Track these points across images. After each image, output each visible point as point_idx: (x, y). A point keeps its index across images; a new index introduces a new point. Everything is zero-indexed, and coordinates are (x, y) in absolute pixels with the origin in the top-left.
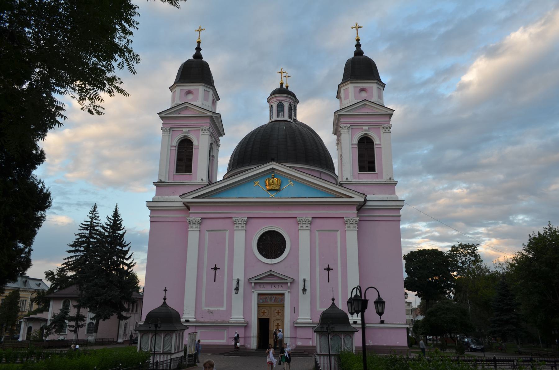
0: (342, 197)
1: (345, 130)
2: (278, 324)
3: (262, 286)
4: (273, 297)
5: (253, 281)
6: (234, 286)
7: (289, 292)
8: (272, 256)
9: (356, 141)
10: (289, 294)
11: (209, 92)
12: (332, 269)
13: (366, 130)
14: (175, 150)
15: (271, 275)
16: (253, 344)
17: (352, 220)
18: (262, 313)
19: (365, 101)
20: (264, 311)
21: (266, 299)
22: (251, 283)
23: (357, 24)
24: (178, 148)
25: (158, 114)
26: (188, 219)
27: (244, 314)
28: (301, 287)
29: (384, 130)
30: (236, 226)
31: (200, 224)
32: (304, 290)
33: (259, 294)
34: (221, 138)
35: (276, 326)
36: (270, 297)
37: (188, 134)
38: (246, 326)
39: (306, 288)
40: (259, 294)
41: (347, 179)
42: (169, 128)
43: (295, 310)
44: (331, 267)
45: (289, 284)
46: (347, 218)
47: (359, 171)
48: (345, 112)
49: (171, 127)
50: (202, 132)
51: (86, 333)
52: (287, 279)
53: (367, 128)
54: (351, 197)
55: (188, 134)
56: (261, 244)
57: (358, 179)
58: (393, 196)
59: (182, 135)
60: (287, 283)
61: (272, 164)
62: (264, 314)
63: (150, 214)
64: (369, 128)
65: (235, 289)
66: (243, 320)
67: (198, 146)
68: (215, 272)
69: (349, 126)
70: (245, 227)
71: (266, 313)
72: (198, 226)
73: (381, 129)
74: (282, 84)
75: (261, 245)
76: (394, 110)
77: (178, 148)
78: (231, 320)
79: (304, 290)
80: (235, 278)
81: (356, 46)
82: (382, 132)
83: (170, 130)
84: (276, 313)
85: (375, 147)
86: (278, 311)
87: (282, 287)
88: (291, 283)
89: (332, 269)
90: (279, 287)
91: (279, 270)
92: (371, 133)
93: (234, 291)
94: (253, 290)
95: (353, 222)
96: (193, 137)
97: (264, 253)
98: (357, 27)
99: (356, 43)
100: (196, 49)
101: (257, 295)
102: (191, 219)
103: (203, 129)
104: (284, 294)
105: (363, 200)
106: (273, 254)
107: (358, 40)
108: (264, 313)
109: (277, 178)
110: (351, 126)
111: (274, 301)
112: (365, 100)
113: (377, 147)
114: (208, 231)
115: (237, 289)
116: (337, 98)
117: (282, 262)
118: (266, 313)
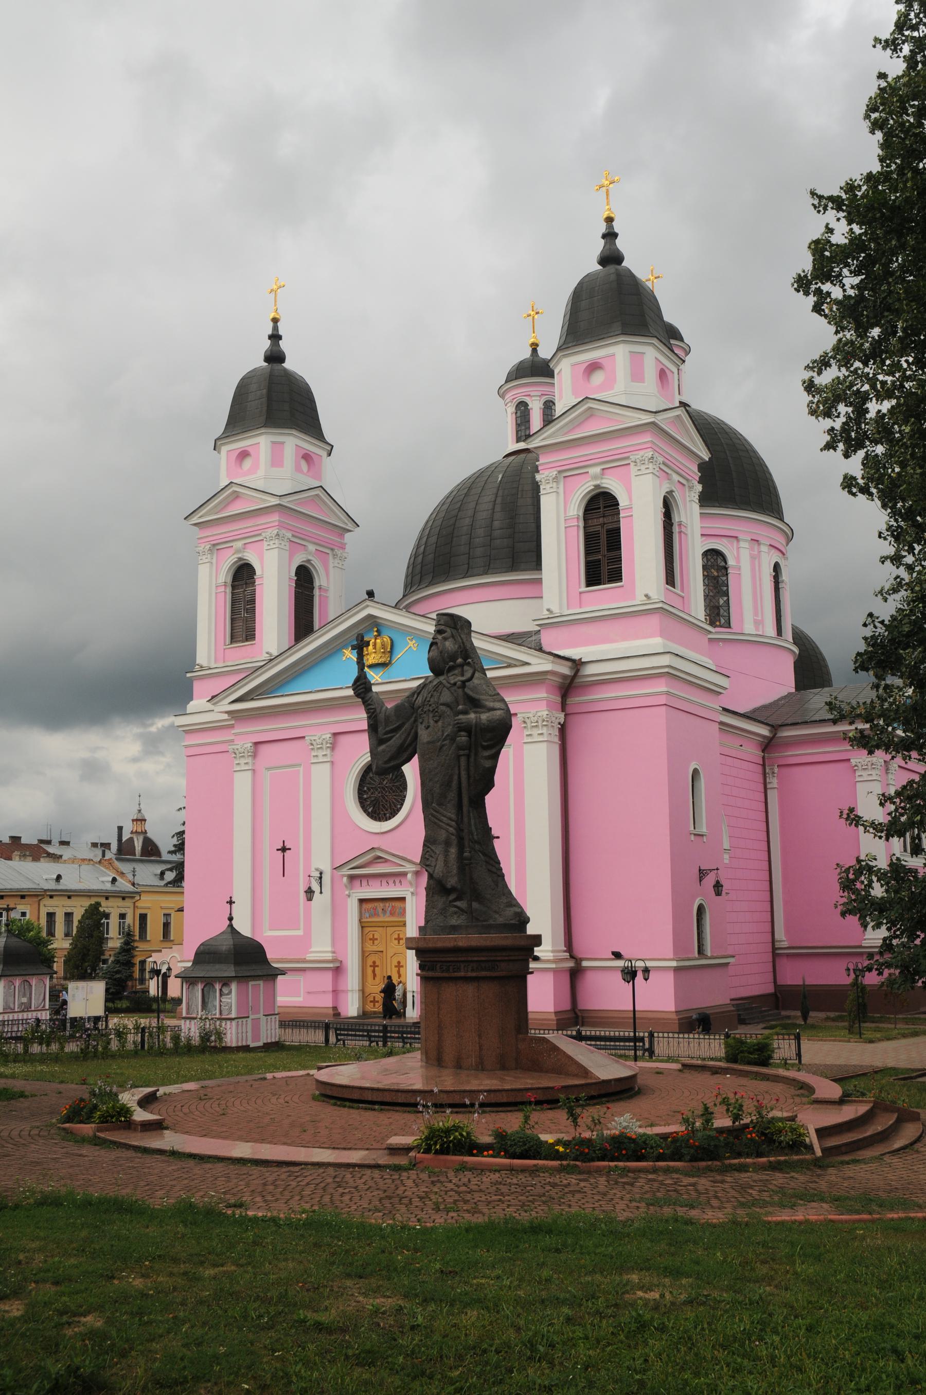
1: (548, 486)
2: (399, 963)
3: (364, 882)
4: (387, 905)
5: (346, 871)
7: (412, 893)
8: (385, 814)
9: (576, 509)
10: (414, 898)
11: (283, 443)
13: (595, 477)
14: (225, 592)
17: (536, 719)
18: (370, 939)
20: (373, 935)
21: (375, 909)
22: (344, 876)
24: (233, 587)
25: (185, 519)
27: (334, 942)
30: (314, 753)
31: (255, 755)
33: (362, 901)
34: (347, 535)
35: (396, 966)
36: (380, 905)
37: (245, 554)
38: (338, 970)
42: (208, 547)
45: (409, 876)
46: (524, 715)
49: (212, 543)
53: (597, 470)
54: (527, 664)
55: (245, 554)
56: (365, 789)
57: (580, 607)
59: (234, 559)
60: (404, 874)
61: (368, 606)
62: (373, 943)
64: (603, 469)
65: (306, 892)
66: (329, 956)
69: (554, 473)
70: (329, 756)
71: (377, 939)
72: (250, 760)
73: (633, 469)
74: (535, 347)
75: (365, 791)
78: (310, 957)
83: (210, 550)
84: (395, 939)
85: (621, 515)
86: (399, 935)
90: (394, 882)
92: (611, 482)
94: (347, 893)
95: (537, 722)
99: (602, 228)
100: (270, 337)
102: (238, 747)
106: (387, 810)
107: (609, 220)
110: (560, 472)
111: (391, 914)
112: (587, 398)
117: (399, 828)
118: (377, 939)
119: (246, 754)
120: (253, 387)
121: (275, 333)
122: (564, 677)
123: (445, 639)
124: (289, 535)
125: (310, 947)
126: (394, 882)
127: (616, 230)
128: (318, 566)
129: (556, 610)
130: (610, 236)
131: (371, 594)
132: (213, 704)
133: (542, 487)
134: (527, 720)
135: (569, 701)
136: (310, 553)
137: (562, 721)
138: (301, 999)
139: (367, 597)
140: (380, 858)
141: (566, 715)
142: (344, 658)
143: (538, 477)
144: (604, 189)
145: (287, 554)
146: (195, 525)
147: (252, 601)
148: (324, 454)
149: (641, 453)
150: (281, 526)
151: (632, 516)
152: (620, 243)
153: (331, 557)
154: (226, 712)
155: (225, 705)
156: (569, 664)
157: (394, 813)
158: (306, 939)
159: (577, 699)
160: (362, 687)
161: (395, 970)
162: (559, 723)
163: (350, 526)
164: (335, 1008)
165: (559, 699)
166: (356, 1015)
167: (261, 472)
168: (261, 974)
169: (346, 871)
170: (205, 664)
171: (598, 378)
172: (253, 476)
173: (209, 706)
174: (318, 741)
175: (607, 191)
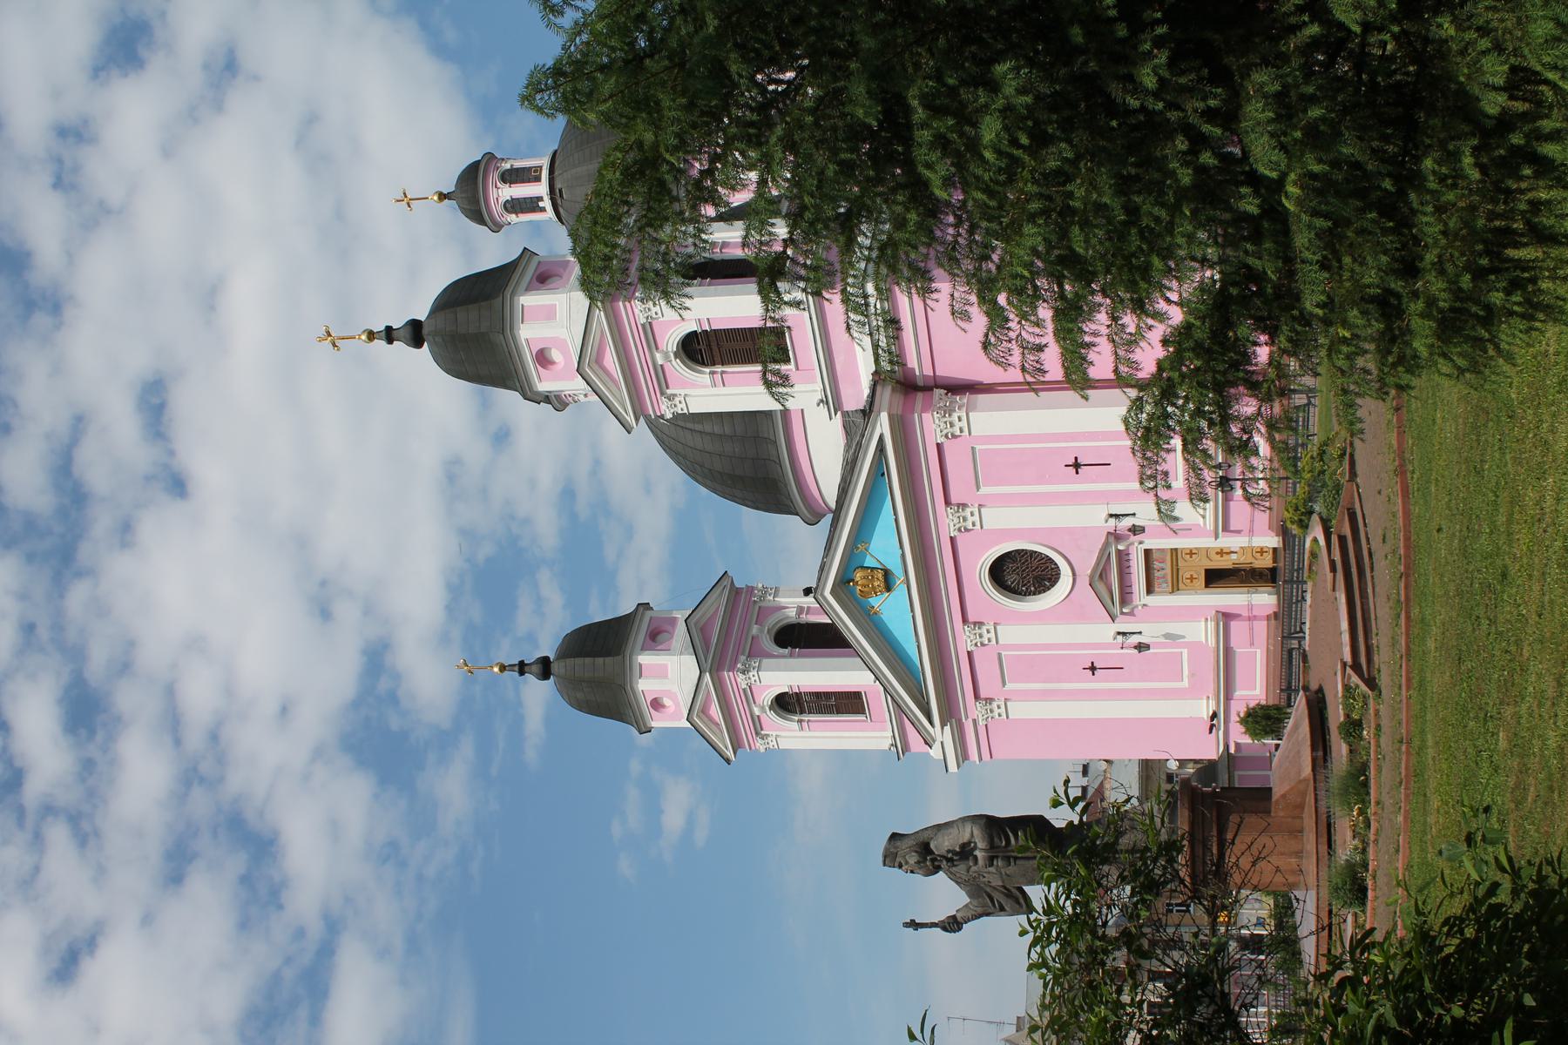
1: (679, 406)
2: (1217, 553)
7: (1141, 543)
9: (703, 376)
12: (1076, 458)
14: (809, 721)
16: (1264, 600)
17: (942, 425)
19: (581, 370)
38: (1226, 617)
42: (760, 740)
44: (1072, 461)
59: (772, 715)
60: (1119, 552)
66: (1211, 625)
77: (801, 713)
78: (1212, 642)
81: (390, 341)
89: (1076, 458)
91: (1087, 565)
95: (946, 422)
96: (767, 697)
101: (1149, 597)
104: (1147, 553)
108: (1192, 579)
110: (662, 393)
114: (1004, 684)
119: (988, 707)
120: (580, 695)
121: (517, 668)
122: (893, 390)
123: (907, 863)
124: (743, 658)
125: (1201, 642)
127: (383, 328)
128: (774, 621)
129: (820, 395)
130: (390, 335)
131: (807, 592)
132: (934, 741)
133: (680, 412)
135: (920, 383)
136: (761, 631)
137: (943, 392)
138: (1259, 651)
139: (812, 595)
140: (1101, 575)
141: (937, 387)
143: (669, 416)
144: (336, 342)
145: (766, 661)
146: (735, 753)
147: (818, 695)
148: (649, 614)
149: (636, 311)
150: (732, 668)
151: (708, 319)
152: (397, 323)
153: (763, 604)
154: (942, 729)
155: (936, 731)
156: (879, 388)
157: (1050, 560)
158: (1194, 647)
159: (917, 373)
160: (952, 925)
161: (1225, 557)
162: (946, 394)
163: (725, 582)
164: (1268, 617)
165: (920, 395)
166: (1275, 597)
167: (675, 689)
168: (1227, 776)
170: (890, 741)
171: (556, 355)
172: (678, 694)
173: (937, 746)
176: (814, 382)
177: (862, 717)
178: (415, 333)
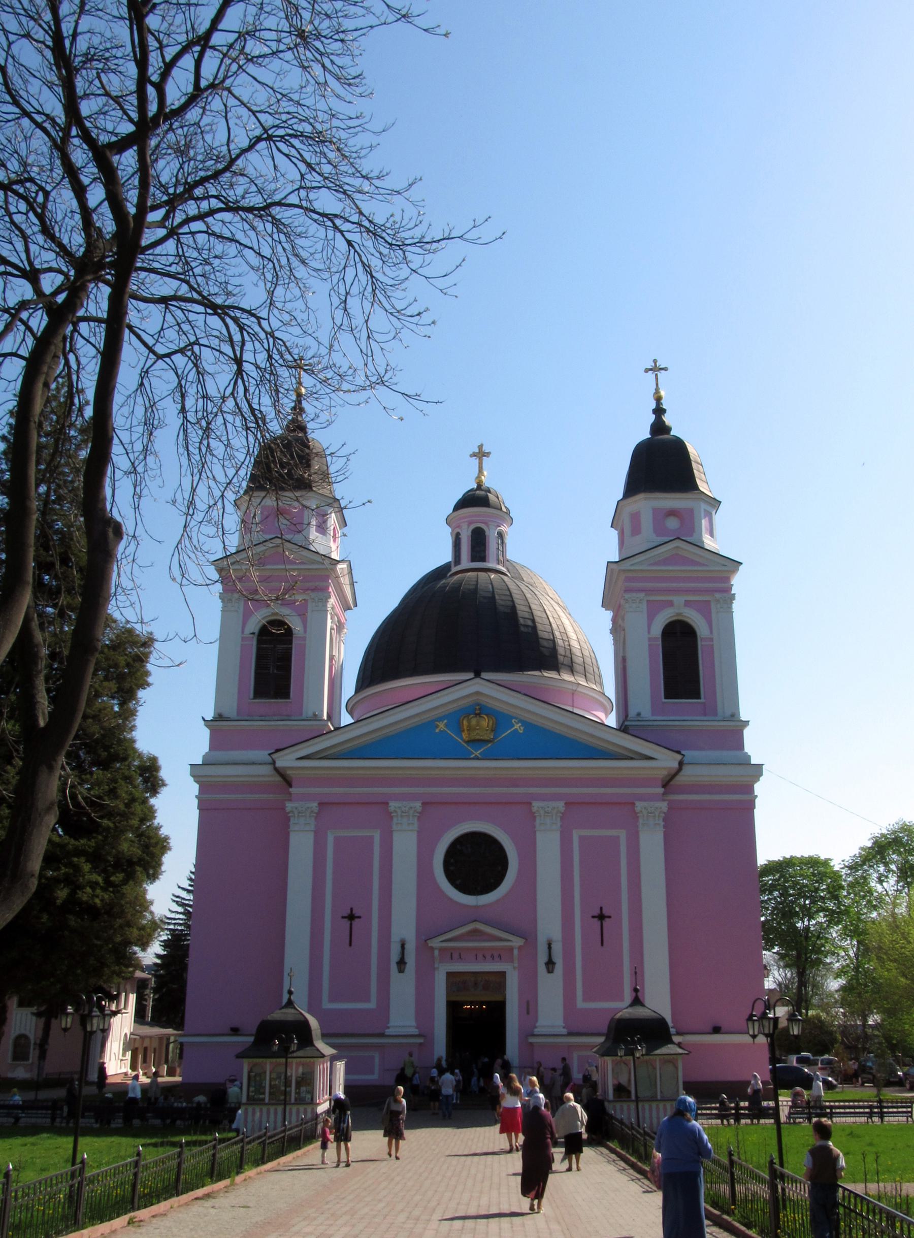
0: (632, 759)
6: (395, 957)
9: (657, 630)
15: (475, 932)
19: (677, 540)
22: (432, 949)
23: (655, 361)
24: (259, 642)
26: (289, 806)
28: (542, 959)
29: (719, 606)
32: (550, 964)
39: (555, 959)
40: (449, 975)
41: (639, 714)
43: (529, 1007)
44: (606, 912)
45: (516, 952)
47: (666, 698)
48: (632, 565)
50: (314, 604)
51: (9, 1061)
52: (511, 939)
58: (738, 753)
60: (511, 949)
63: (197, 794)
66: (415, 1031)
67: (304, 639)
68: (351, 925)
76: (741, 563)
79: (550, 964)
80: (395, 938)
82: (713, 611)
87: (500, 956)
88: (520, 948)
89: (609, 917)
90: (492, 956)
93: (394, 967)
97: (458, 882)
98: (656, 369)
99: (653, 405)
101: (445, 975)
103: (317, 599)
104: (503, 974)
105: (676, 765)
107: (658, 399)
109: (486, 715)
113: (703, 643)
115: (402, 963)
116: (612, 527)
126: (492, 956)
130: (659, 411)
134: (643, 810)
142: (437, 731)
169: (435, 943)
174: (404, 809)
175: (656, 375)
176: (653, 714)
177: (252, 695)
178: (659, 427)
